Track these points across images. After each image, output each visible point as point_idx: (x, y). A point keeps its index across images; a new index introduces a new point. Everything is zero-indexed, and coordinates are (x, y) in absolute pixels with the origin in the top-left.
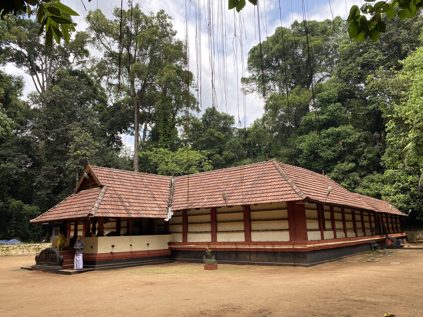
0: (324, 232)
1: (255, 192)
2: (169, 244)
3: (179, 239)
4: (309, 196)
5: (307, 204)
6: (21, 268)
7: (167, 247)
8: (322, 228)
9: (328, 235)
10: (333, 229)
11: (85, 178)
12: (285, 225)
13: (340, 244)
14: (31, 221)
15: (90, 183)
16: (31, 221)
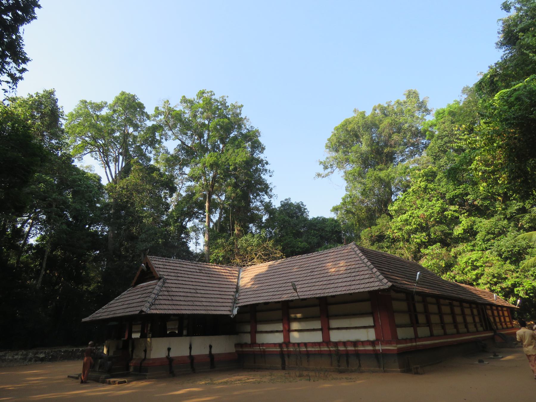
0: (418, 329)
1: (332, 282)
2: (237, 345)
3: (247, 339)
4: (395, 284)
5: (393, 294)
6: (68, 377)
7: (233, 350)
8: (414, 323)
9: (423, 331)
10: (429, 324)
11: (143, 270)
12: (369, 321)
13: (439, 343)
14: (83, 320)
15: (148, 275)
16: (83, 320)
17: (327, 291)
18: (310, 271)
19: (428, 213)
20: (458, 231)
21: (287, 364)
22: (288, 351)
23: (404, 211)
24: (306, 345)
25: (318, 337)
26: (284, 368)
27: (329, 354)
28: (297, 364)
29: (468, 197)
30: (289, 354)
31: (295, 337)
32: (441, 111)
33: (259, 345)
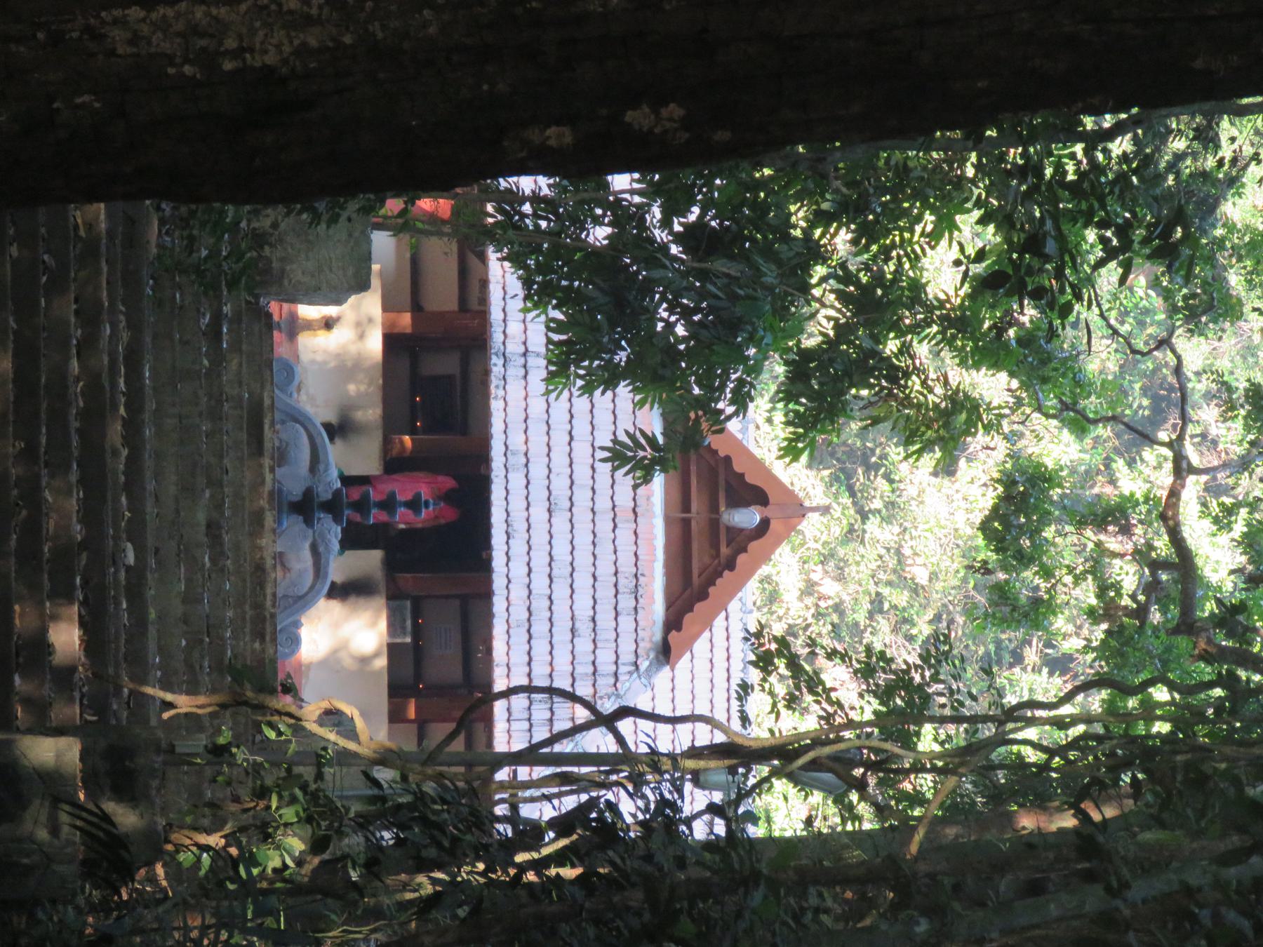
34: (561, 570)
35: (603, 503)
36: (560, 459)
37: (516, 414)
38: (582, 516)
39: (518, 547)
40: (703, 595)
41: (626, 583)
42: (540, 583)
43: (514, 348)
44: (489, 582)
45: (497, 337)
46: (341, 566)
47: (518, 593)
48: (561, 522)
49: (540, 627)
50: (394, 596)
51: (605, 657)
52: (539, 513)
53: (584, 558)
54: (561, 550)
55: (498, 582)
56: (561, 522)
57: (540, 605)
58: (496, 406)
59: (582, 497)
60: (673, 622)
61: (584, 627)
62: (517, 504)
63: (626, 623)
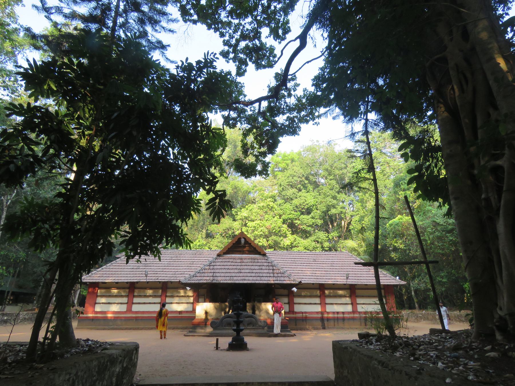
17: (362, 281)
18: (330, 265)
19: (272, 226)
20: (287, 242)
21: (326, 325)
22: (327, 317)
23: (250, 219)
24: (343, 313)
25: (349, 308)
26: (324, 328)
27: (360, 318)
28: (334, 325)
29: (297, 221)
30: (328, 319)
31: (329, 308)
32: (287, 155)
33: (296, 313)
34: (251, 271)
35: (240, 264)
36: (232, 271)
37: (224, 278)
38: (242, 267)
39: (247, 278)
40: (255, 248)
41: (253, 261)
42: (253, 275)
43: (212, 278)
44: (253, 284)
45: (209, 281)
46: (249, 311)
47: (255, 278)
48: (242, 271)
49: (261, 275)
50: (254, 301)
51: (265, 264)
52: (241, 275)
53: (249, 267)
54: (247, 271)
55: (253, 282)
56: (242, 271)
57: (257, 275)
58: (221, 282)
59: (238, 267)
60: (259, 253)
61: (261, 267)
62: (239, 278)
63: (259, 261)
